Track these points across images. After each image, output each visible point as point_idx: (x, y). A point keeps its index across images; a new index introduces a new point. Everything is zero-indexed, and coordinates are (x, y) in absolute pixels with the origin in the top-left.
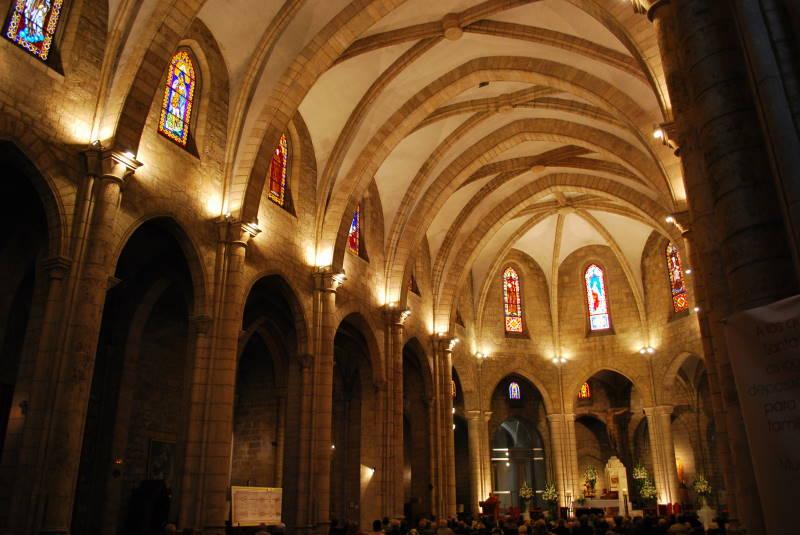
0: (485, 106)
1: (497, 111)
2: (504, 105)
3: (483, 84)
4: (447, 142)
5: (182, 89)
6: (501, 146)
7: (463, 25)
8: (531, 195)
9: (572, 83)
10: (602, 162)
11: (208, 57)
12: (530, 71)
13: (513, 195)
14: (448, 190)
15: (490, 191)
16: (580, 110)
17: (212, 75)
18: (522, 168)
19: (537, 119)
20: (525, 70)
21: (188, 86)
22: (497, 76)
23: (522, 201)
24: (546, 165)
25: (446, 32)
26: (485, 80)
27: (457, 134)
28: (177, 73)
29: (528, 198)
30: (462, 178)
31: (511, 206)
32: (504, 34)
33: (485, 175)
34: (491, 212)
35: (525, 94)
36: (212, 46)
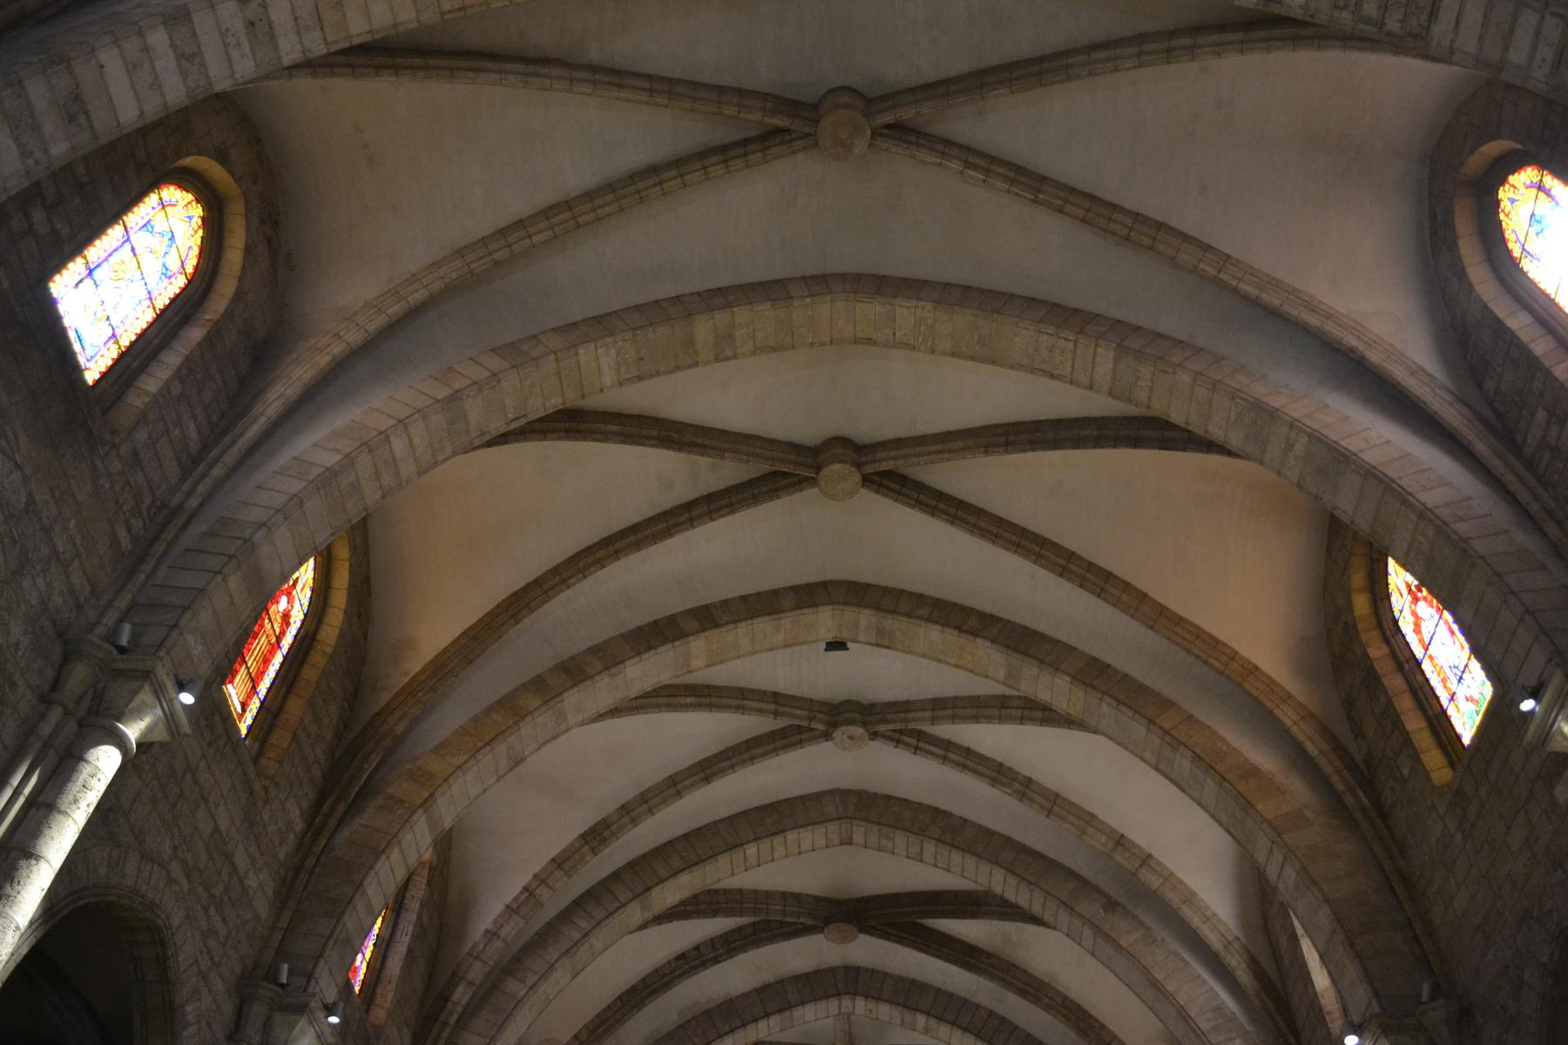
0: (805, 713)
1: (827, 736)
2: (851, 722)
3: (836, 645)
4: (674, 786)
5: (152, 267)
6: (791, 836)
7: (870, 469)
8: (790, 1007)
9: (1075, 678)
10: (989, 955)
11: (249, 250)
12: (974, 633)
13: (746, 995)
14: (634, 914)
15: (703, 965)
16: (1016, 785)
17: (238, 295)
18: (809, 922)
19: (889, 798)
20: (960, 629)
21: (168, 275)
22: (881, 632)
23: (767, 1015)
24: (862, 930)
25: (825, 472)
26: (844, 635)
27: (708, 769)
28: (160, 222)
29: (780, 1011)
30: (670, 894)
31: (738, 1023)
32: (953, 519)
33: (714, 913)
34: (682, 1026)
35: (907, 711)
36: (269, 240)
